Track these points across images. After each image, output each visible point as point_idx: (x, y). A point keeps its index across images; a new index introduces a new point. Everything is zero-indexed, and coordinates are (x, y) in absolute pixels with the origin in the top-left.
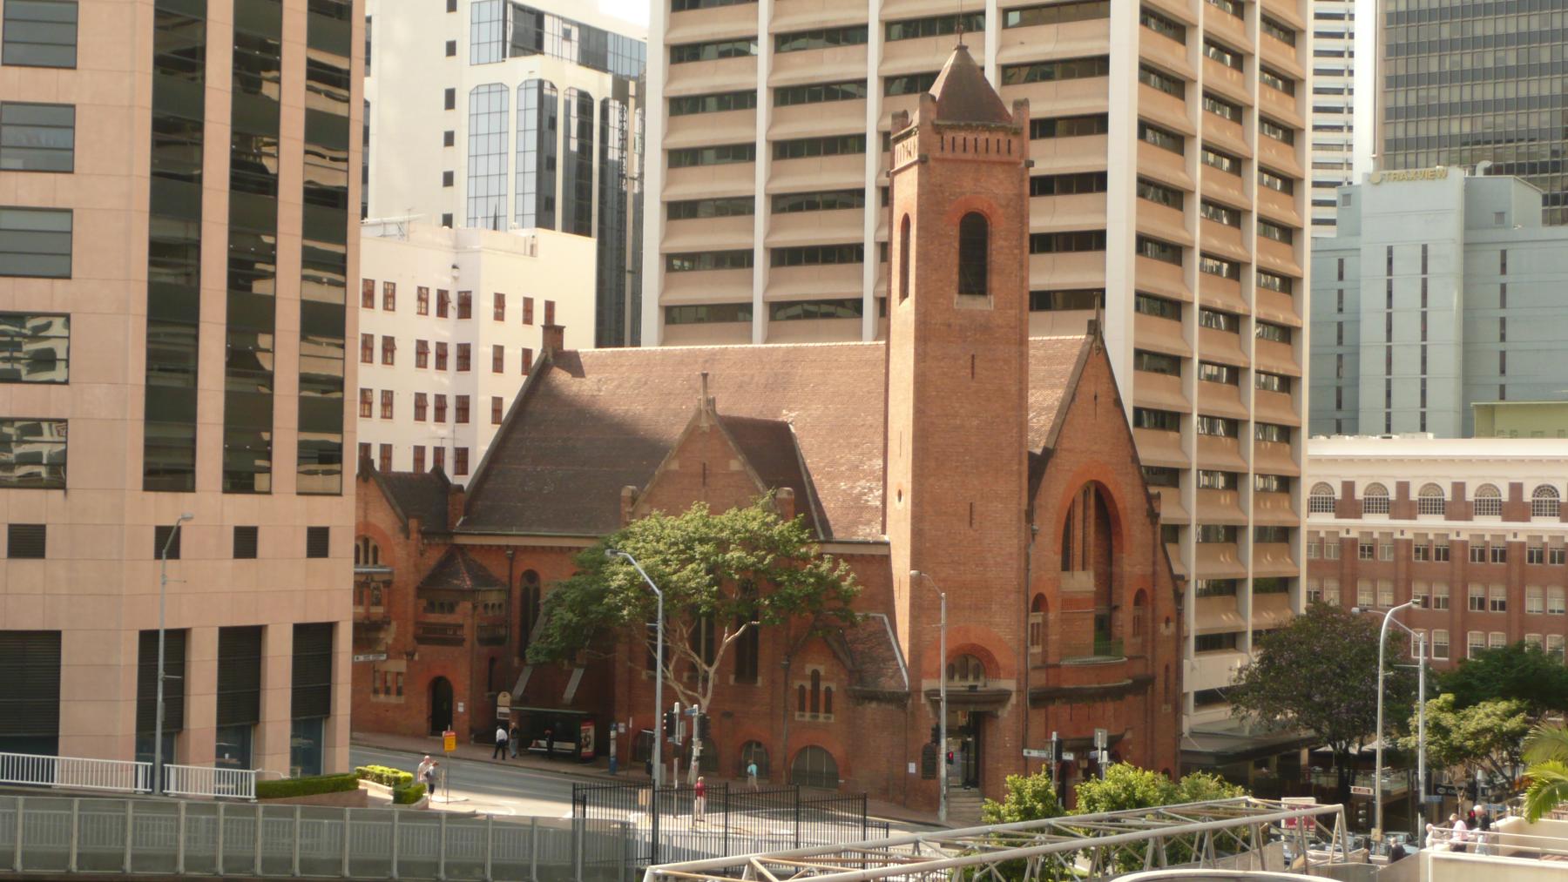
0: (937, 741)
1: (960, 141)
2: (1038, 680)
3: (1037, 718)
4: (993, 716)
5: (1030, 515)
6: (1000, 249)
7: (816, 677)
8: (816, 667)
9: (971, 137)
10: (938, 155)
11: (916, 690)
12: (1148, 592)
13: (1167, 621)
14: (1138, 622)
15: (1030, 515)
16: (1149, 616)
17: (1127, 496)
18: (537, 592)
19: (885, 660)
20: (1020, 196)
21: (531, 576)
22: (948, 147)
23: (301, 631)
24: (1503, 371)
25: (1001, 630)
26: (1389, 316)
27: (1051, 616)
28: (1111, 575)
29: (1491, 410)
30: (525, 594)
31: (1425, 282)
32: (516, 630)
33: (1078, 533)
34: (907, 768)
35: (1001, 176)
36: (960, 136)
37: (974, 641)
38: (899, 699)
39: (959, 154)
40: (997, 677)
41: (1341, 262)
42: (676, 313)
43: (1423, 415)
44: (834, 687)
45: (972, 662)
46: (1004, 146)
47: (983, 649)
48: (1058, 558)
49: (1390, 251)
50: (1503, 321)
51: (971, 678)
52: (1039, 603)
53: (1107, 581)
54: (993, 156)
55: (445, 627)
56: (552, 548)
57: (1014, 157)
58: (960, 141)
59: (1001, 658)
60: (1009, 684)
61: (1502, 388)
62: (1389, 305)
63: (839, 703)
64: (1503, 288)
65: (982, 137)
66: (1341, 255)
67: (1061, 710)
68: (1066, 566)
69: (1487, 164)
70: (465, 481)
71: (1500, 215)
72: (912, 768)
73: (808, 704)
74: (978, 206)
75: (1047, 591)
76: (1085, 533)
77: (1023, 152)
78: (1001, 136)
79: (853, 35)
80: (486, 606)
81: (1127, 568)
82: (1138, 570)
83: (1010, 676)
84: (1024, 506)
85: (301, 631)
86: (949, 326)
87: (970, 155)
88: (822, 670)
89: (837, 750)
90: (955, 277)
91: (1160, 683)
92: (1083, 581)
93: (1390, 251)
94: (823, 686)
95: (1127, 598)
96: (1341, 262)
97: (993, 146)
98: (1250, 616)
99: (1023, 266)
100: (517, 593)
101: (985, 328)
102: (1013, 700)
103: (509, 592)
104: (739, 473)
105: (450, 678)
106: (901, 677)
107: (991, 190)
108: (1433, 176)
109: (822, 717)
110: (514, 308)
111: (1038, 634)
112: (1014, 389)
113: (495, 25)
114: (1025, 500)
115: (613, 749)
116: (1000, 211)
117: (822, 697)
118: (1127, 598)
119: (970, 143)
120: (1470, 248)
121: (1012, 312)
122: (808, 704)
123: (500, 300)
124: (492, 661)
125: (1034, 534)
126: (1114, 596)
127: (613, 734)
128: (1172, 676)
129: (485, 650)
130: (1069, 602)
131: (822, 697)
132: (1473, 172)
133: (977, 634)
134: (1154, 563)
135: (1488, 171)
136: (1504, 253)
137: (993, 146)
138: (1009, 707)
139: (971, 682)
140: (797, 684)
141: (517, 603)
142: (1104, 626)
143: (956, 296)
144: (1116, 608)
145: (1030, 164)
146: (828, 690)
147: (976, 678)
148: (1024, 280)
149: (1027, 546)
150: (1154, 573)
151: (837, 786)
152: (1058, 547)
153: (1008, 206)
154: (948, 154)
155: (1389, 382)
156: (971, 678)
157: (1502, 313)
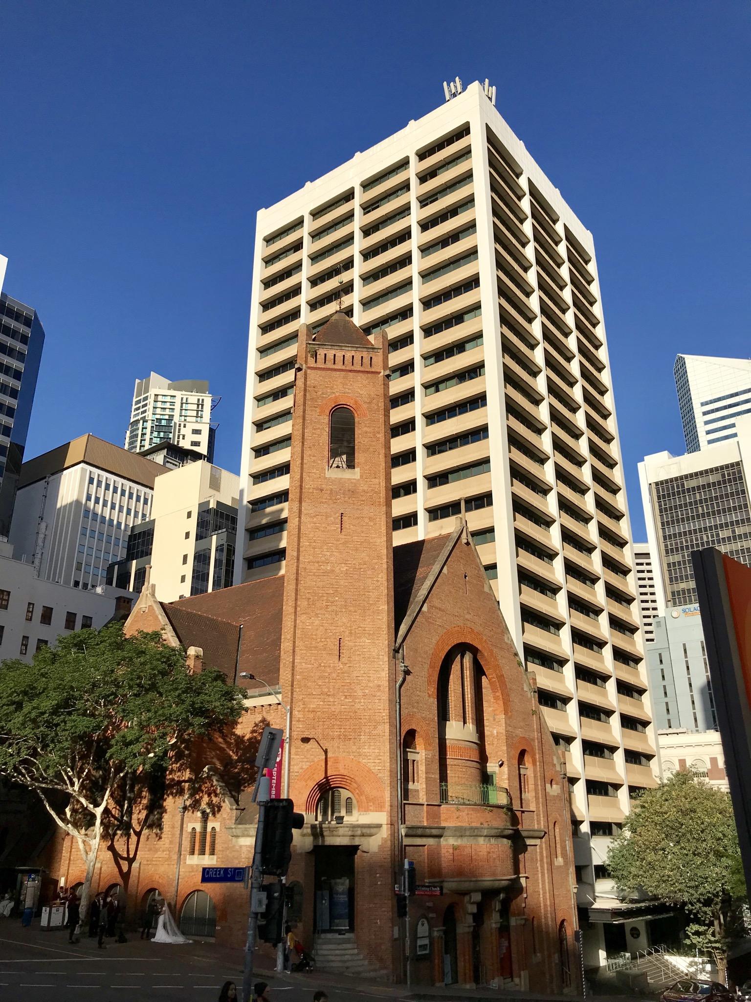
1: (330, 356)
6: (367, 433)
35: (365, 382)
36: (330, 353)
41: (660, 655)
46: (366, 361)
49: (684, 645)
54: (358, 367)
58: (330, 356)
66: (660, 651)
83: (380, 808)
86: (322, 490)
93: (684, 645)
96: (660, 655)
101: (352, 492)
116: (365, 406)
119: (339, 359)
140: (188, 828)
152: (433, 689)
154: (320, 364)
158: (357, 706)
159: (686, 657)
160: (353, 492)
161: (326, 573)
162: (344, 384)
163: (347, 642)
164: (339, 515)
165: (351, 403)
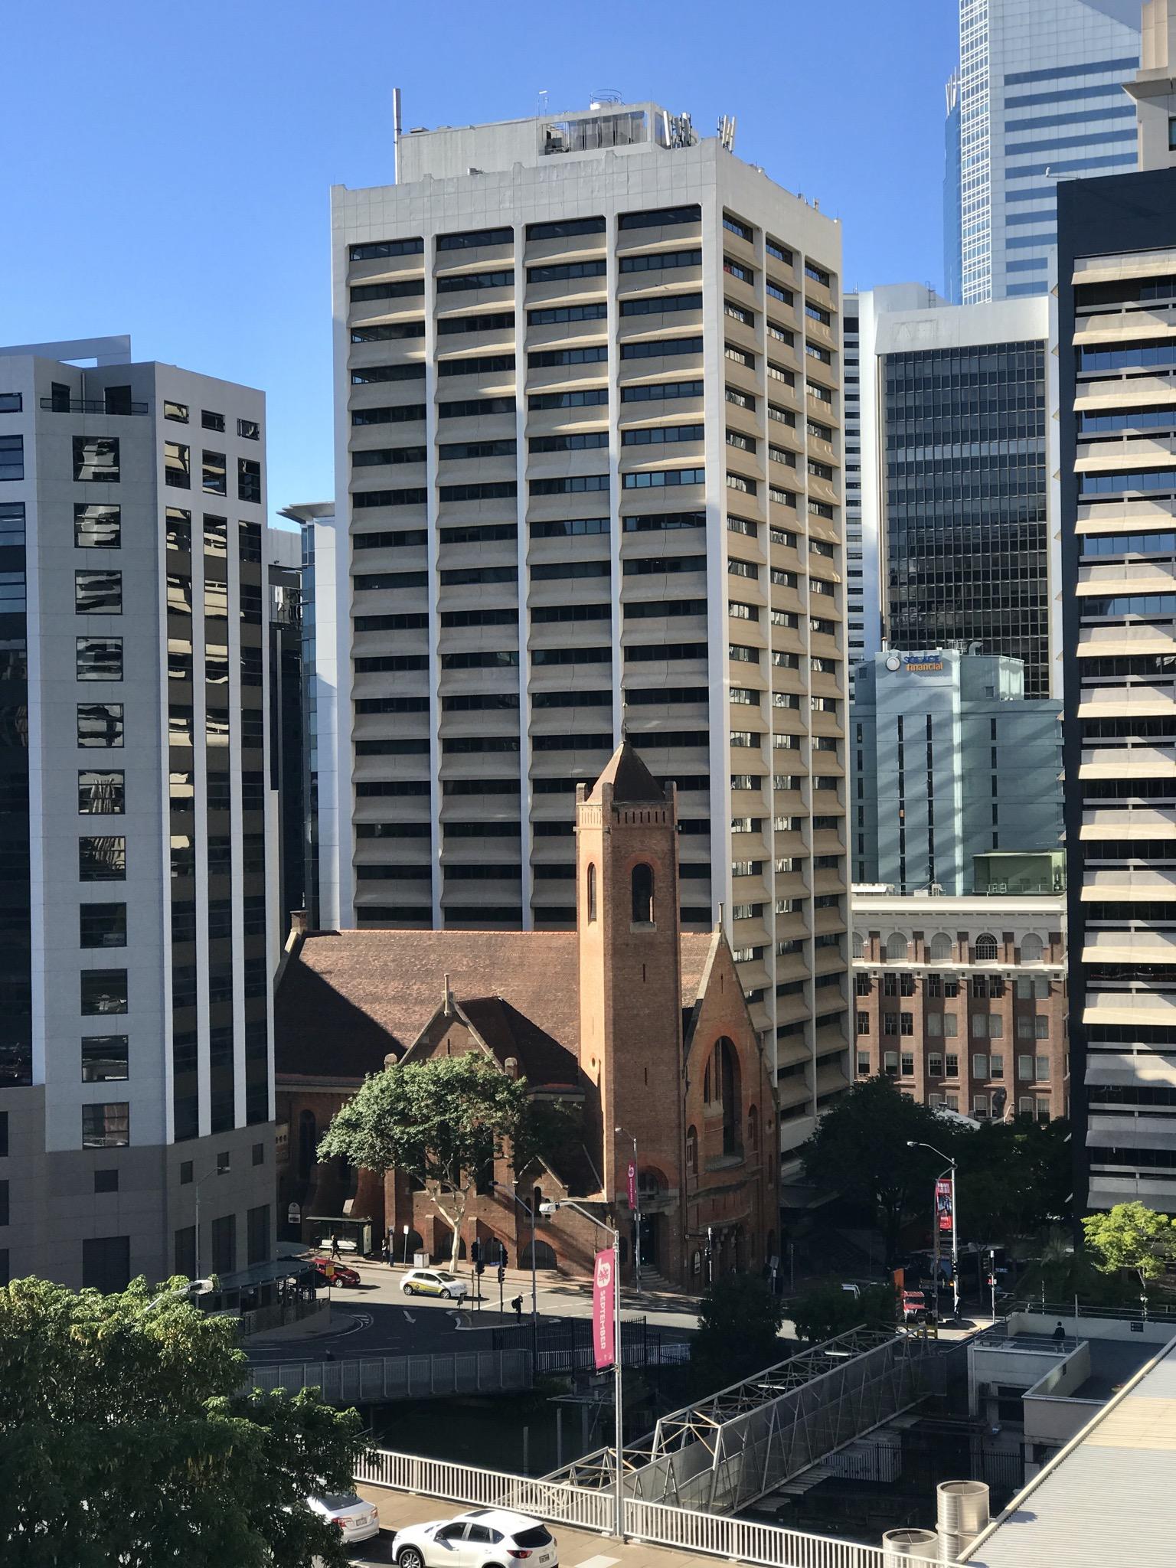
13: (770, 1123)
14: (754, 1129)
17: (744, 1043)
22: (622, 821)
23: (252, 1213)
27: (699, 1139)
47: (661, 1172)
68: (707, 1099)
74: (646, 858)
75: (697, 1122)
85: (252, 1213)
90: (630, 911)
92: (717, 1108)
95: (745, 1112)
97: (653, 819)
98: (815, 1085)
107: (651, 848)
112: (672, 986)
118: (745, 1112)
130: (709, 1124)
135: (978, 650)
147: (652, 1189)
162: (642, 842)
163: (651, 1070)
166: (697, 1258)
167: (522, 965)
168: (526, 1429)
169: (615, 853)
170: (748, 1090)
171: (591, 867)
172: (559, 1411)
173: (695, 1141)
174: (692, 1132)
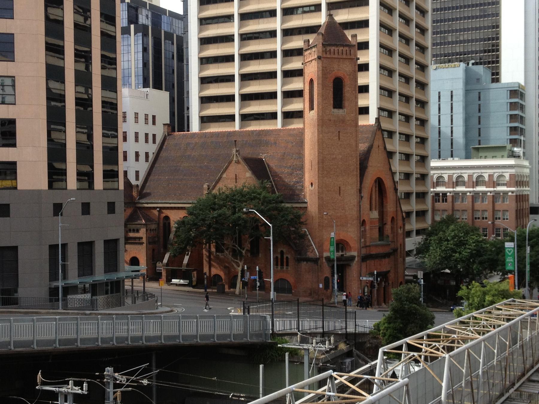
0: (333, 276)
2: (364, 251)
3: (364, 265)
4: (349, 265)
5: (360, 191)
7: (282, 253)
8: (282, 249)
9: (336, 49)
10: (325, 56)
11: (321, 257)
12: (395, 217)
14: (392, 228)
15: (360, 191)
16: (395, 226)
18: (169, 223)
19: (308, 246)
20: (355, 71)
21: (167, 218)
24: (480, 135)
25: (351, 234)
26: (439, 116)
27: (367, 228)
28: (383, 212)
29: (477, 149)
30: (164, 224)
31: (452, 104)
32: (161, 240)
33: (374, 197)
34: (319, 285)
35: (348, 64)
36: (332, 48)
37: (342, 238)
38: (315, 261)
39: (333, 56)
40: (350, 251)
42: (205, 119)
43: (452, 151)
44: (289, 256)
45: (340, 246)
46: (348, 52)
48: (369, 206)
49: (439, 93)
50: (479, 117)
51: (340, 251)
52: (363, 223)
53: (382, 214)
54: (344, 56)
55: (135, 238)
56: (175, 207)
57: (352, 57)
59: (351, 244)
60: (355, 253)
61: (479, 141)
62: (439, 113)
63: (291, 263)
64: (479, 105)
65: (341, 49)
67: (371, 262)
68: (371, 209)
69: (473, 61)
70: (140, 183)
71: (478, 80)
72: (321, 286)
73: (279, 263)
74: (340, 74)
76: (375, 196)
77: (356, 55)
78: (347, 48)
79: (272, 13)
80: (151, 230)
81: (389, 209)
82: (392, 210)
83: (355, 251)
84: (359, 188)
86: (330, 120)
87: (336, 56)
88: (285, 251)
89: (291, 280)
91: (399, 250)
92: (375, 214)
93: (439, 93)
94: (285, 257)
95: (389, 219)
97: (344, 52)
99: (356, 98)
100: (161, 225)
102: (356, 259)
103: (158, 224)
104: (250, 177)
105: (138, 257)
106: (315, 252)
108: (455, 67)
109: (285, 267)
110: (141, 118)
111: (363, 234)
113: (124, 12)
114: (359, 185)
115: (205, 282)
116: (348, 77)
117: (285, 260)
119: (336, 52)
120: (467, 92)
121: (353, 115)
122: (279, 263)
123: (137, 114)
124: (153, 250)
125: (362, 198)
126: (384, 220)
127: (205, 276)
128: (402, 247)
129: (151, 246)
131: (285, 260)
132: (468, 64)
133: (342, 236)
134: (397, 207)
135: (473, 64)
136: (479, 93)
137: (344, 52)
138: (355, 262)
139: (340, 253)
141: (162, 228)
142: (381, 230)
143: (332, 109)
144: (385, 224)
145: (359, 59)
146: (287, 258)
147: (342, 251)
148: (357, 102)
149: (360, 202)
150: (397, 211)
151: (291, 293)
152: (369, 202)
153: (350, 75)
155: (439, 140)
156: (340, 251)
157: (479, 114)
158: (347, 213)
159: (439, 101)
160: (343, 121)
161: (333, 159)
163: (342, 188)
164: (337, 132)
165: (342, 76)
166: (366, 290)
167: (275, 143)
168: (261, 366)
169: (324, 72)
170: (390, 207)
171: (311, 81)
172: (287, 354)
173: (365, 228)
174: (363, 223)
